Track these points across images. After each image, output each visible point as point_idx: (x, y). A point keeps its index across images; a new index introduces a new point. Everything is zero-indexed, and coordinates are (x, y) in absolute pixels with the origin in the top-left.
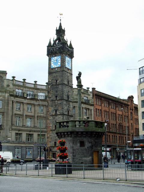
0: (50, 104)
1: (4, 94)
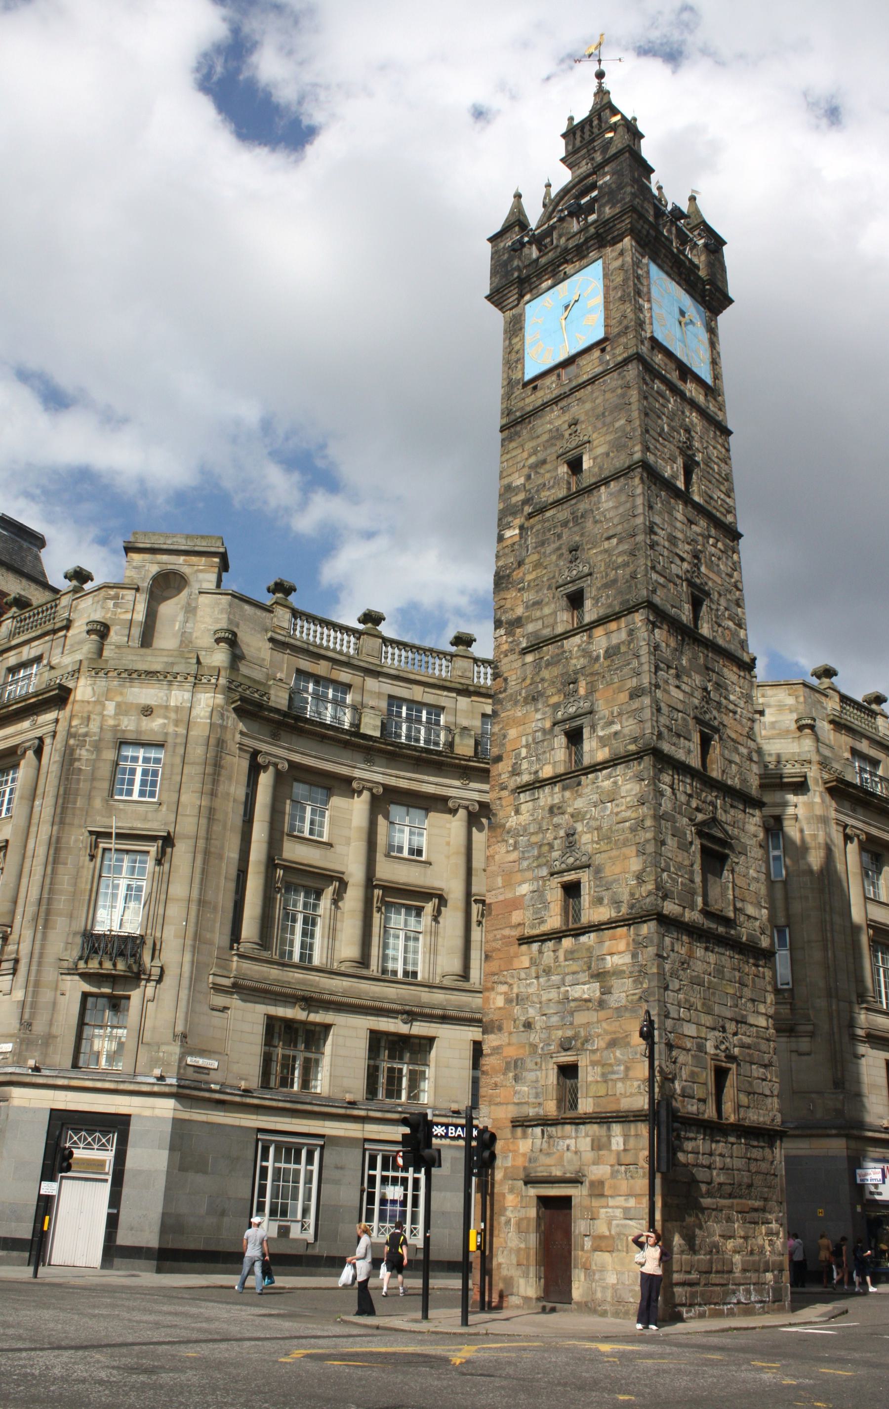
1: (179, 696)
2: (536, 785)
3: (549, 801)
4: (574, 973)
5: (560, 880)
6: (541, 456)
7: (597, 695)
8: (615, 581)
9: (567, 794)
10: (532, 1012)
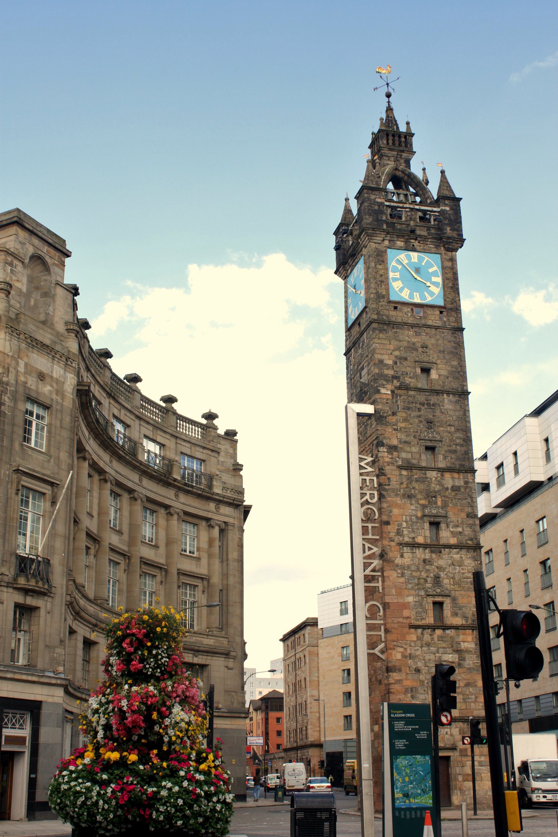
0: (394, 483)
2: (414, 545)
3: (423, 556)
4: (444, 648)
5: (433, 599)
6: (404, 355)
7: (449, 509)
8: (455, 452)
9: (434, 556)
10: (420, 664)
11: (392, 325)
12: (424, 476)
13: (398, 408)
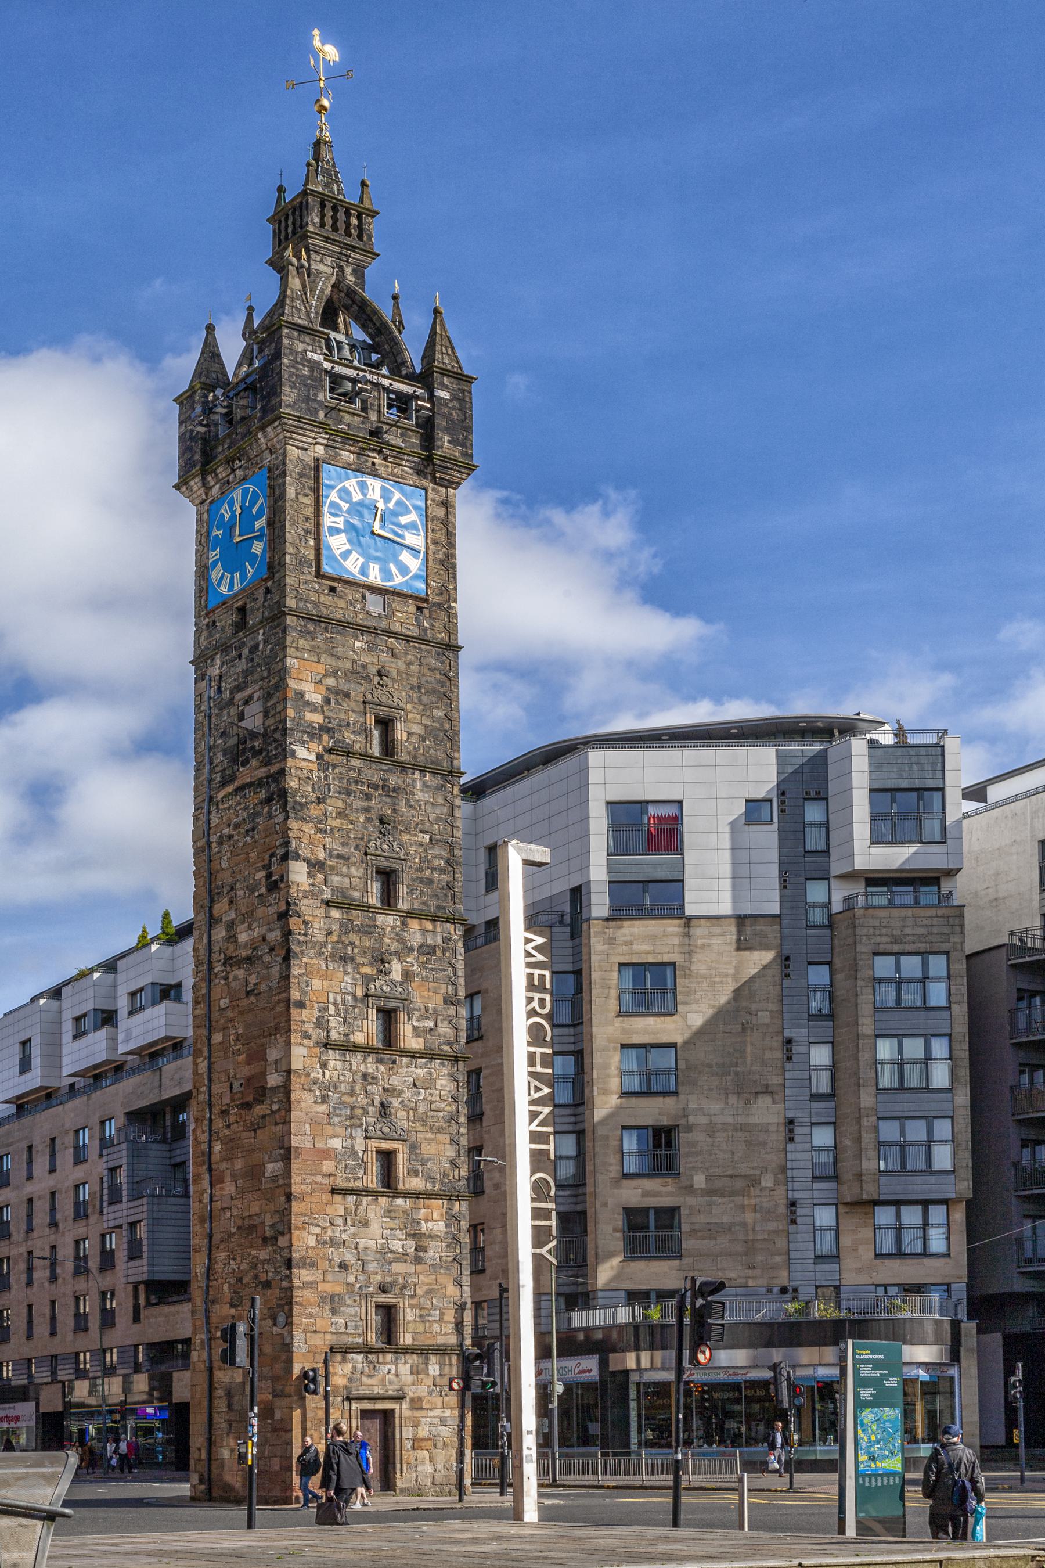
2: (347, 1047)
4: (391, 1229)
5: (377, 1145)
6: (344, 686)
10: (349, 1257)
11: (323, 625)
12: (372, 923)
13: (329, 790)
